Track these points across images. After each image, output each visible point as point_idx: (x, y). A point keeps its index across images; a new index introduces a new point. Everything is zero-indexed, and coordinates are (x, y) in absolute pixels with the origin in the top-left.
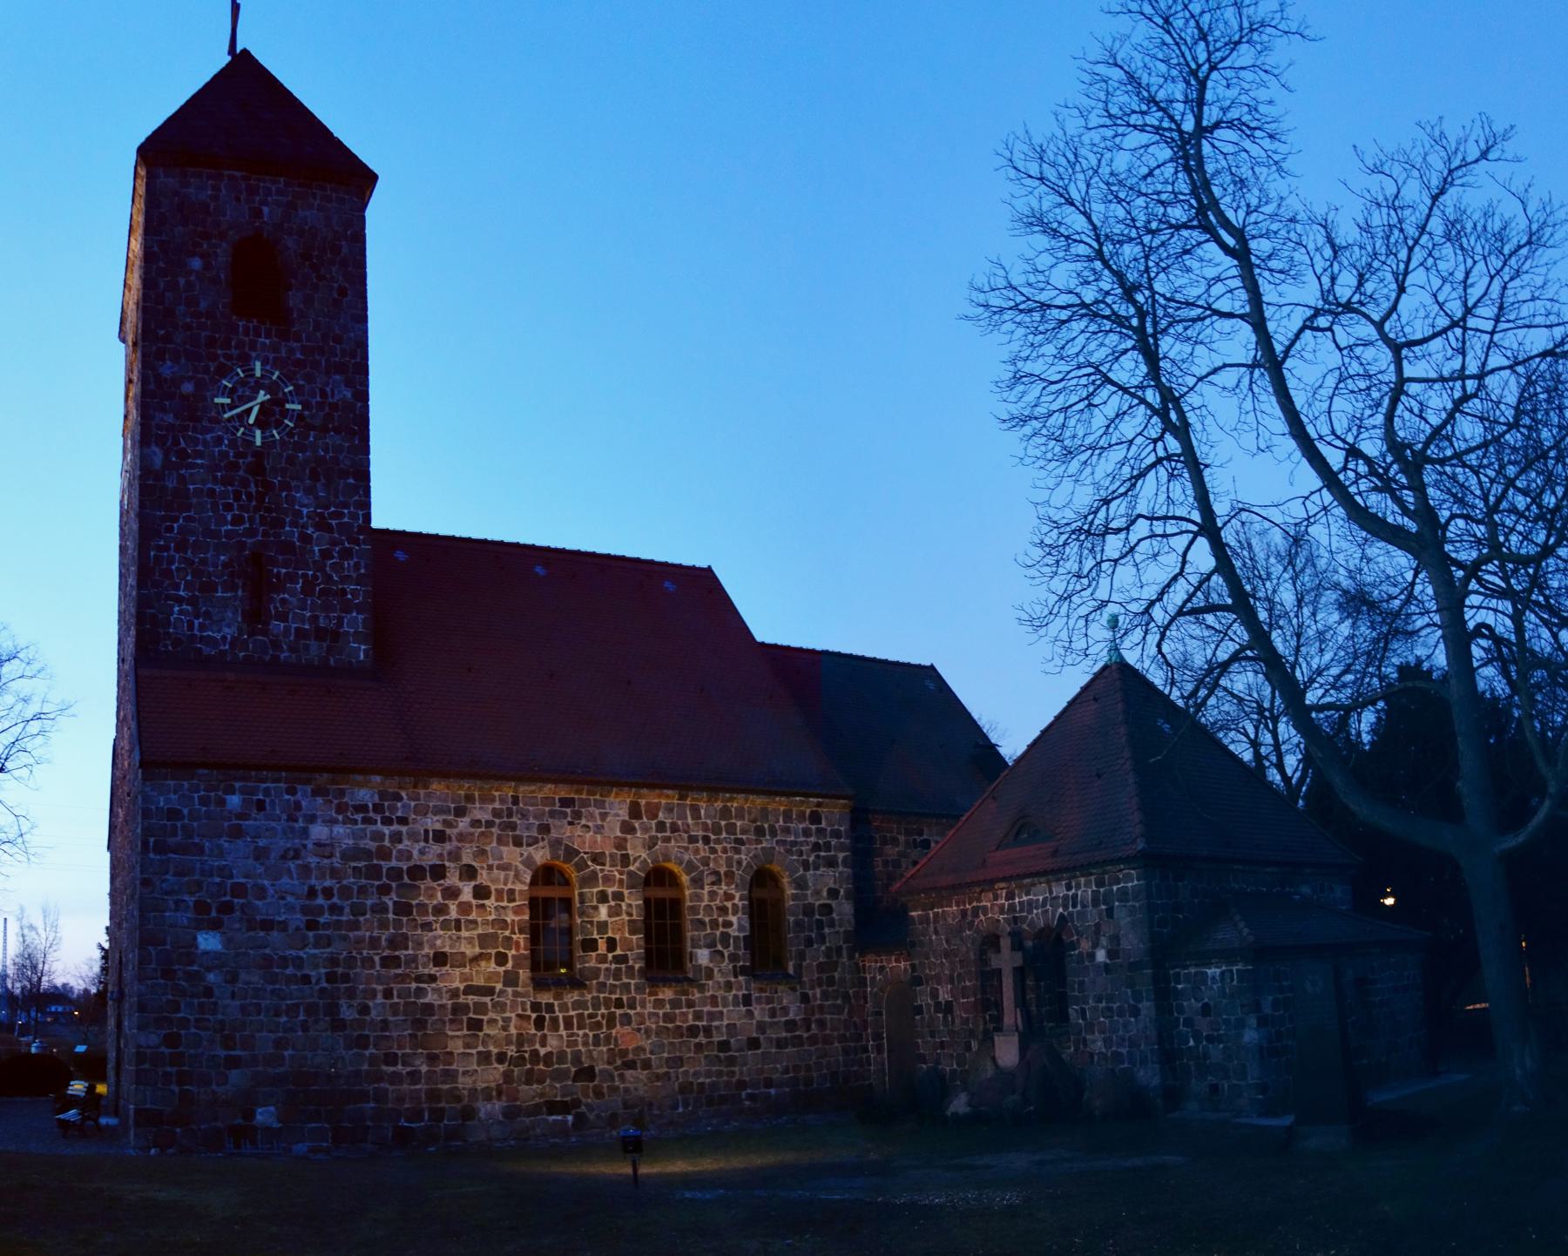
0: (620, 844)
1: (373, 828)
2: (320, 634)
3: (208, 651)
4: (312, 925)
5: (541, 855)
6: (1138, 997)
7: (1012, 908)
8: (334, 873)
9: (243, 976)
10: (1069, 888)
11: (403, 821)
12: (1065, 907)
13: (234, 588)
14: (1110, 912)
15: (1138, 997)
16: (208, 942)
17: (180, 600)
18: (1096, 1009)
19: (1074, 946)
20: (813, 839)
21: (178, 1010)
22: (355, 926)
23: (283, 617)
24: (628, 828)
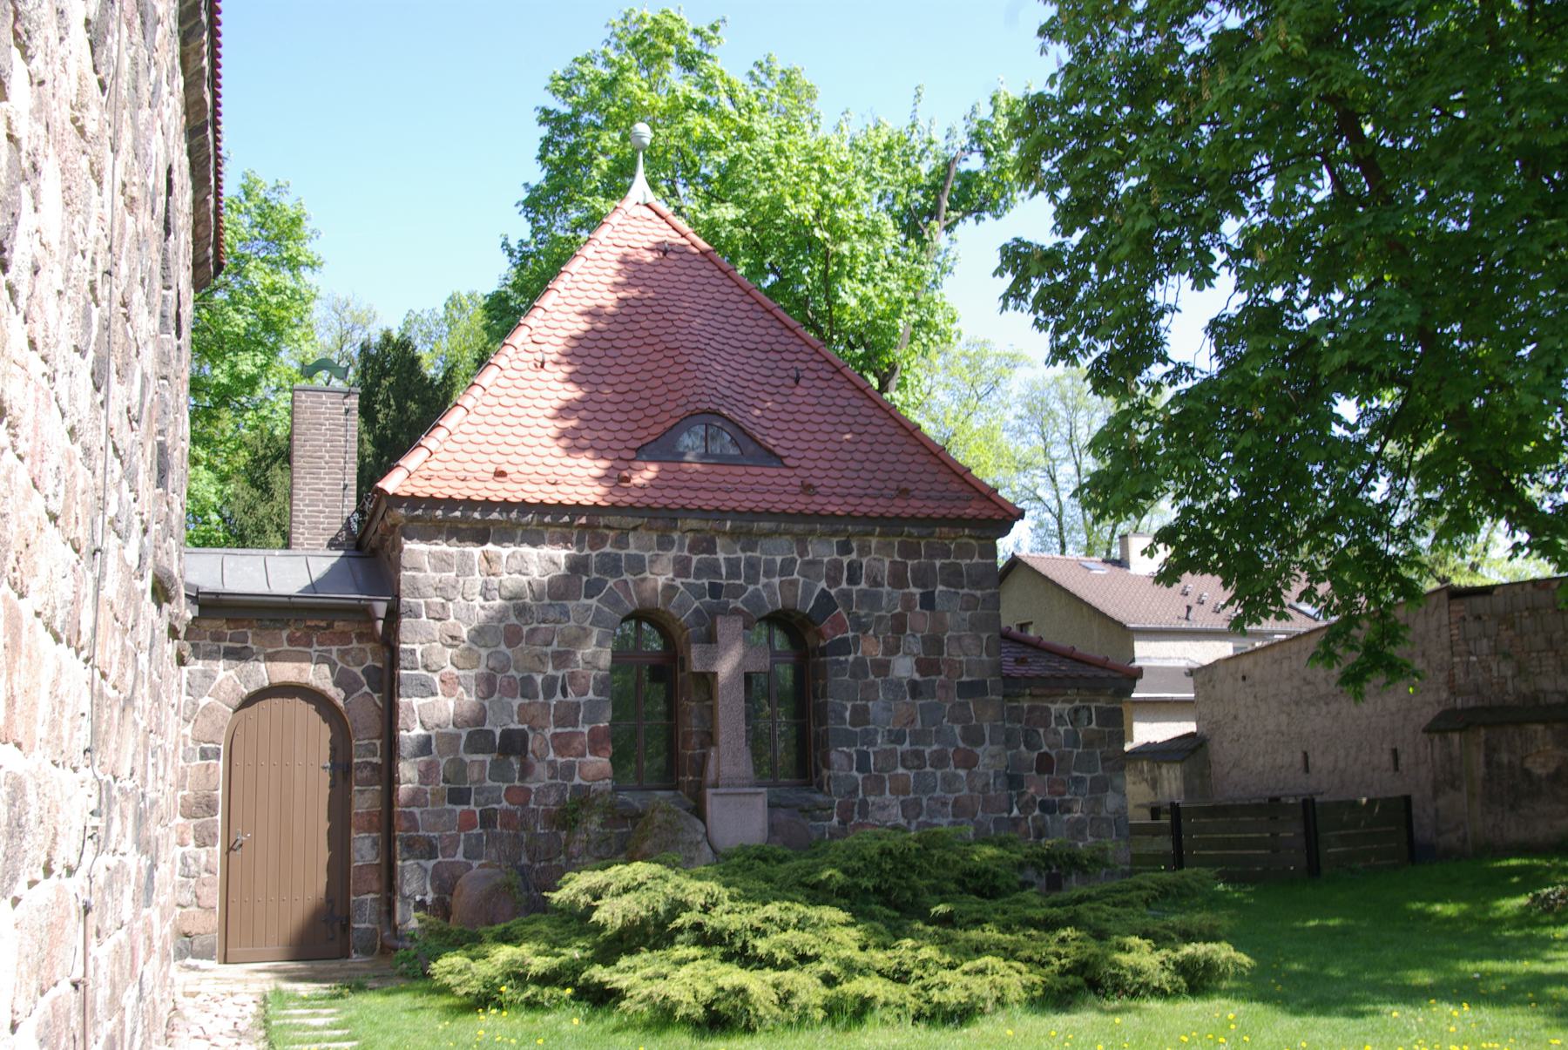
6: (974, 736)
7: (711, 569)
10: (845, 549)
12: (834, 580)
14: (928, 601)
15: (974, 736)
18: (893, 752)
19: (844, 647)
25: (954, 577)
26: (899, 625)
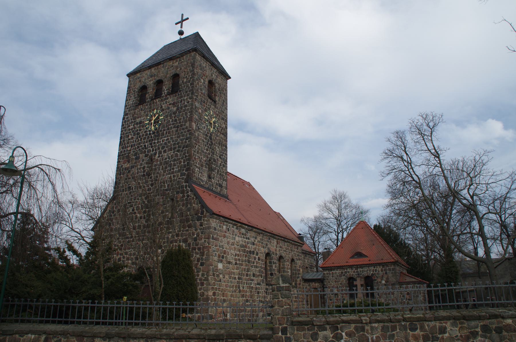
2: (221, 186)
7: (357, 272)
10: (374, 268)
12: (373, 272)
14: (386, 273)
16: (220, 266)
17: (197, 167)
19: (375, 280)
22: (242, 265)
25: (390, 270)
26: (383, 276)
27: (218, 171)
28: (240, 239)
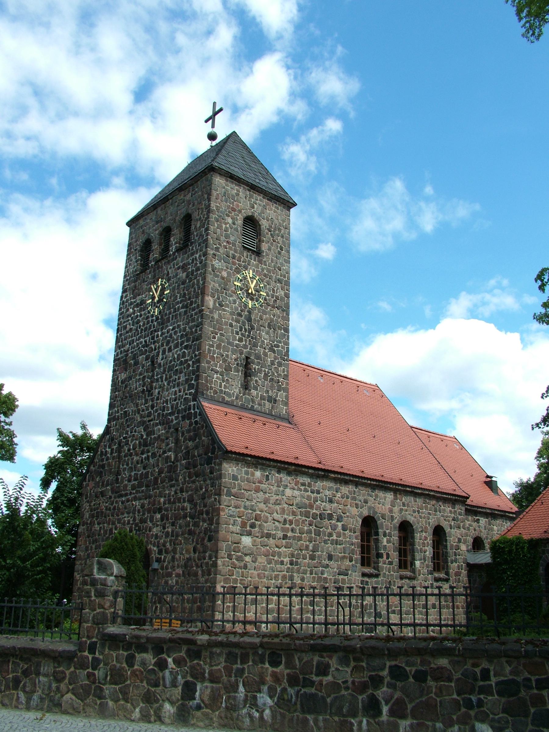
0: (391, 511)
1: (307, 493)
2: (270, 399)
3: (227, 398)
4: (285, 537)
5: (366, 513)
8: (294, 514)
9: (259, 559)
11: (318, 492)
13: (238, 371)
16: (247, 541)
17: (217, 372)
20: (453, 515)
21: (233, 575)
22: (300, 539)
23: (256, 389)
24: (393, 505)
27: (266, 375)
28: (297, 493)
